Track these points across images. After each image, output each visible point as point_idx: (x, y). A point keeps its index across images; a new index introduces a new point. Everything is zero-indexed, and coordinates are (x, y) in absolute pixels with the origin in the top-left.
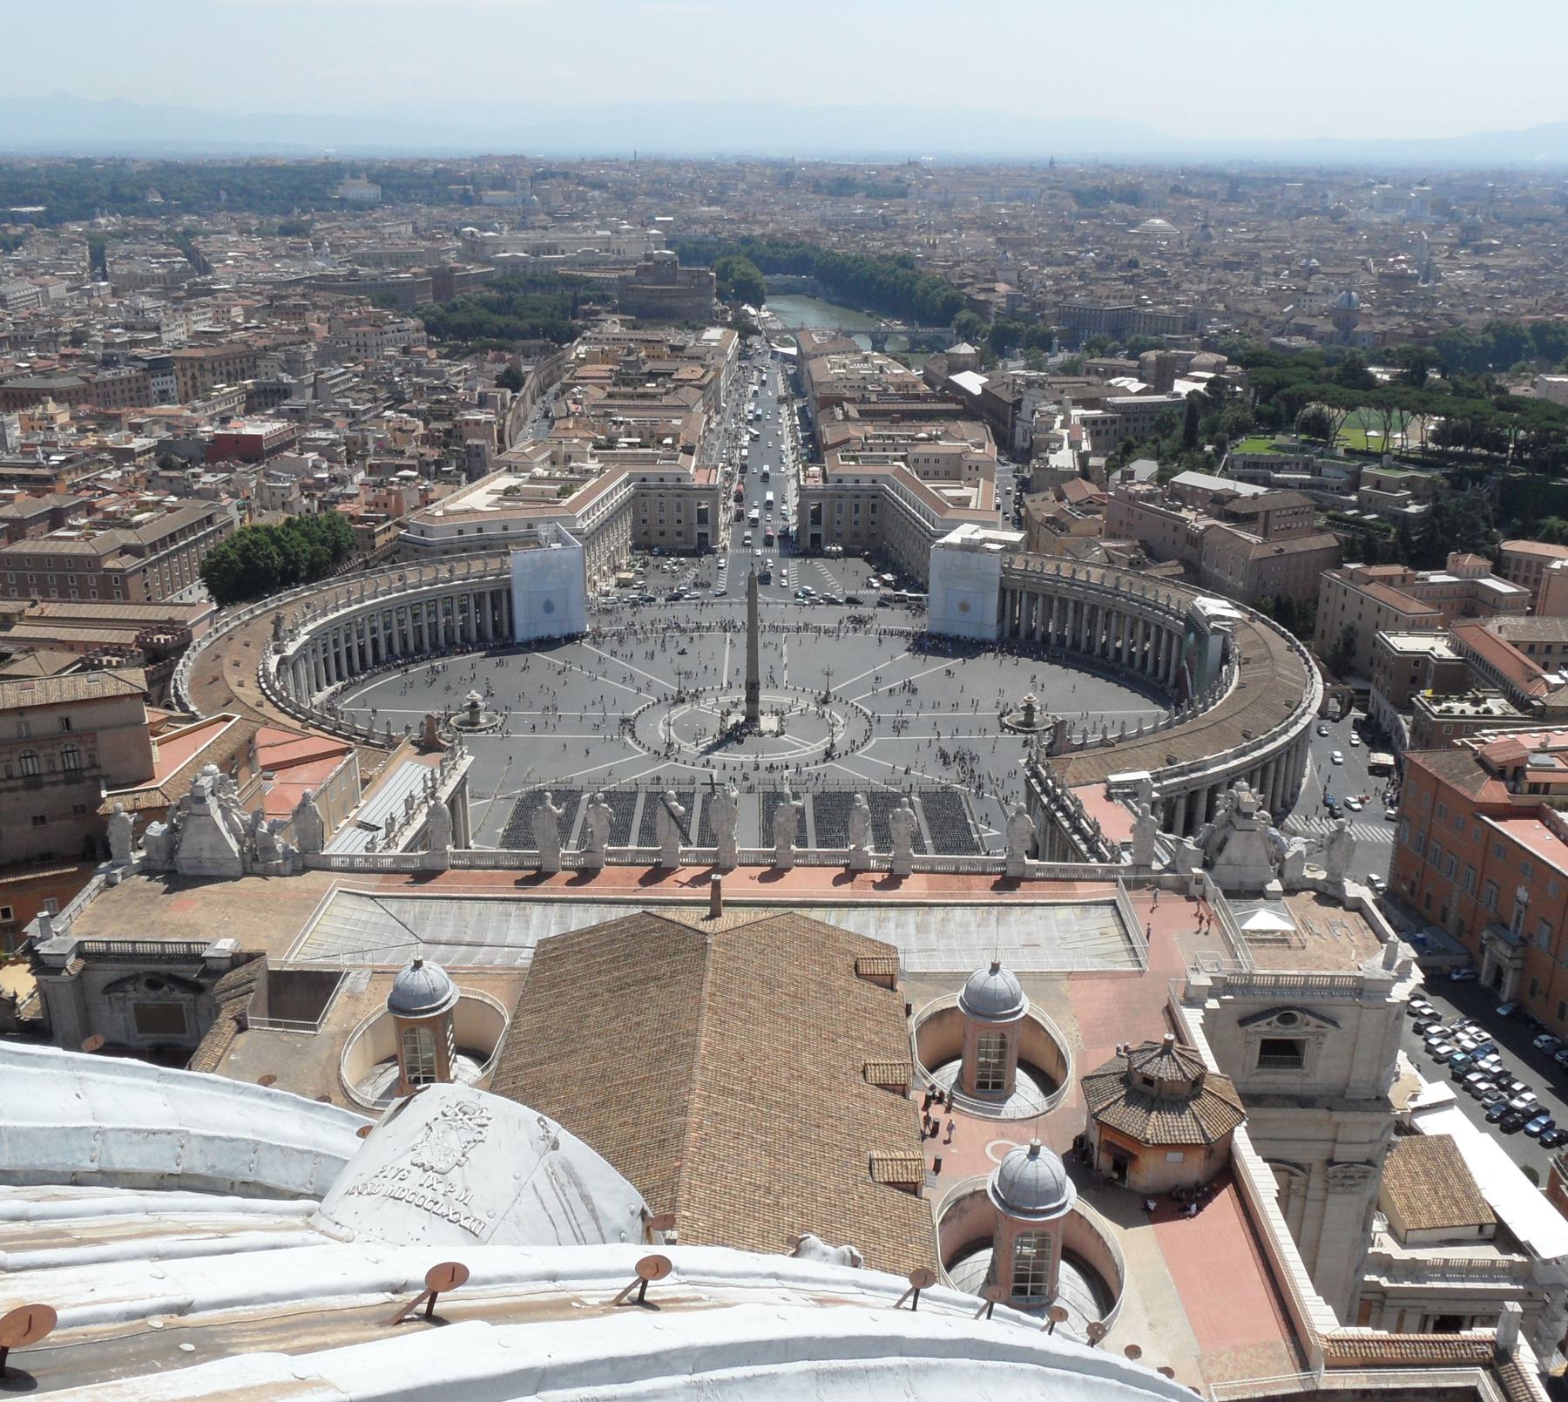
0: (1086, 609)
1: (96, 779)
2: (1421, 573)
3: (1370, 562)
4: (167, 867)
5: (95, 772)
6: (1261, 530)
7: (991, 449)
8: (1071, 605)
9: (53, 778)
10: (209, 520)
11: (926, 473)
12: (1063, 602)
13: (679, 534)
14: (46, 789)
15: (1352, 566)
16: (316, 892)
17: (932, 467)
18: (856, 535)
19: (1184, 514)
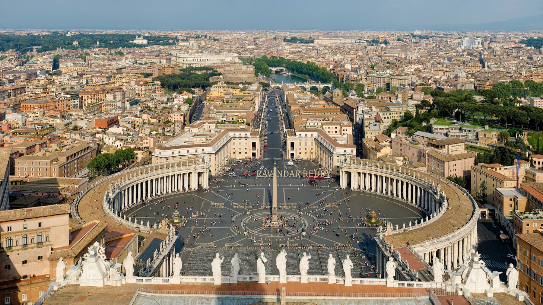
0: (389, 179)
1: (48, 245)
2: (506, 167)
3: (487, 163)
4: (76, 283)
5: (48, 243)
6: (447, 152)
7: (350, 123)
8: (384, 178)
9: (33, 245)
10: (88, 148)
11: (329, 132)
12: (381, 177)
13: (246, 153)
14: (30, 250)
15: (481, 164)
16: (131, 293)
17: (331, 130)
18: (306, 153)
19: (419, 146)
